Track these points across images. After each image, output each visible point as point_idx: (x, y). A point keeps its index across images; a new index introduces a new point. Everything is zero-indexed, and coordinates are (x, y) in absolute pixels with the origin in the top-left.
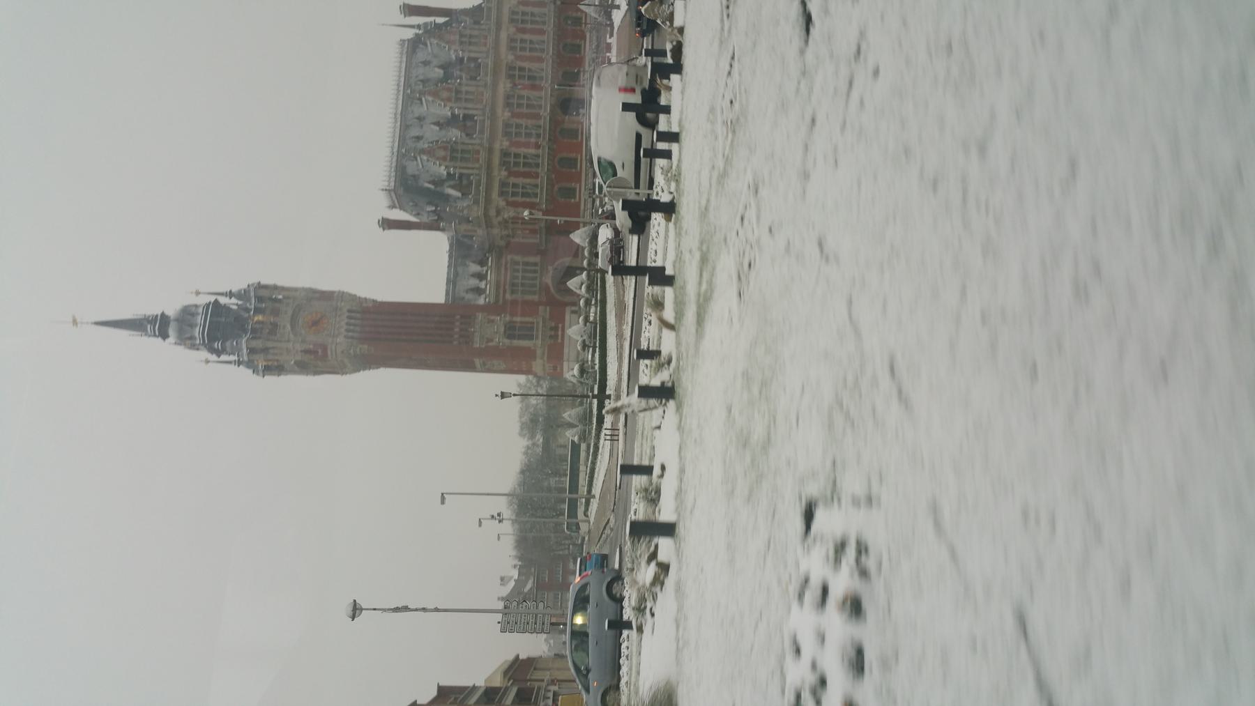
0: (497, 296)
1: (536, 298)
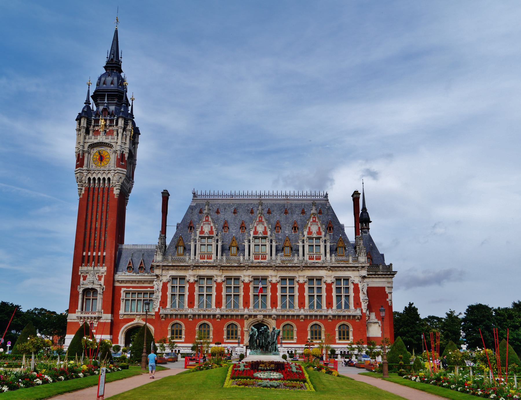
0: (122, 282)
1: (122, 312)
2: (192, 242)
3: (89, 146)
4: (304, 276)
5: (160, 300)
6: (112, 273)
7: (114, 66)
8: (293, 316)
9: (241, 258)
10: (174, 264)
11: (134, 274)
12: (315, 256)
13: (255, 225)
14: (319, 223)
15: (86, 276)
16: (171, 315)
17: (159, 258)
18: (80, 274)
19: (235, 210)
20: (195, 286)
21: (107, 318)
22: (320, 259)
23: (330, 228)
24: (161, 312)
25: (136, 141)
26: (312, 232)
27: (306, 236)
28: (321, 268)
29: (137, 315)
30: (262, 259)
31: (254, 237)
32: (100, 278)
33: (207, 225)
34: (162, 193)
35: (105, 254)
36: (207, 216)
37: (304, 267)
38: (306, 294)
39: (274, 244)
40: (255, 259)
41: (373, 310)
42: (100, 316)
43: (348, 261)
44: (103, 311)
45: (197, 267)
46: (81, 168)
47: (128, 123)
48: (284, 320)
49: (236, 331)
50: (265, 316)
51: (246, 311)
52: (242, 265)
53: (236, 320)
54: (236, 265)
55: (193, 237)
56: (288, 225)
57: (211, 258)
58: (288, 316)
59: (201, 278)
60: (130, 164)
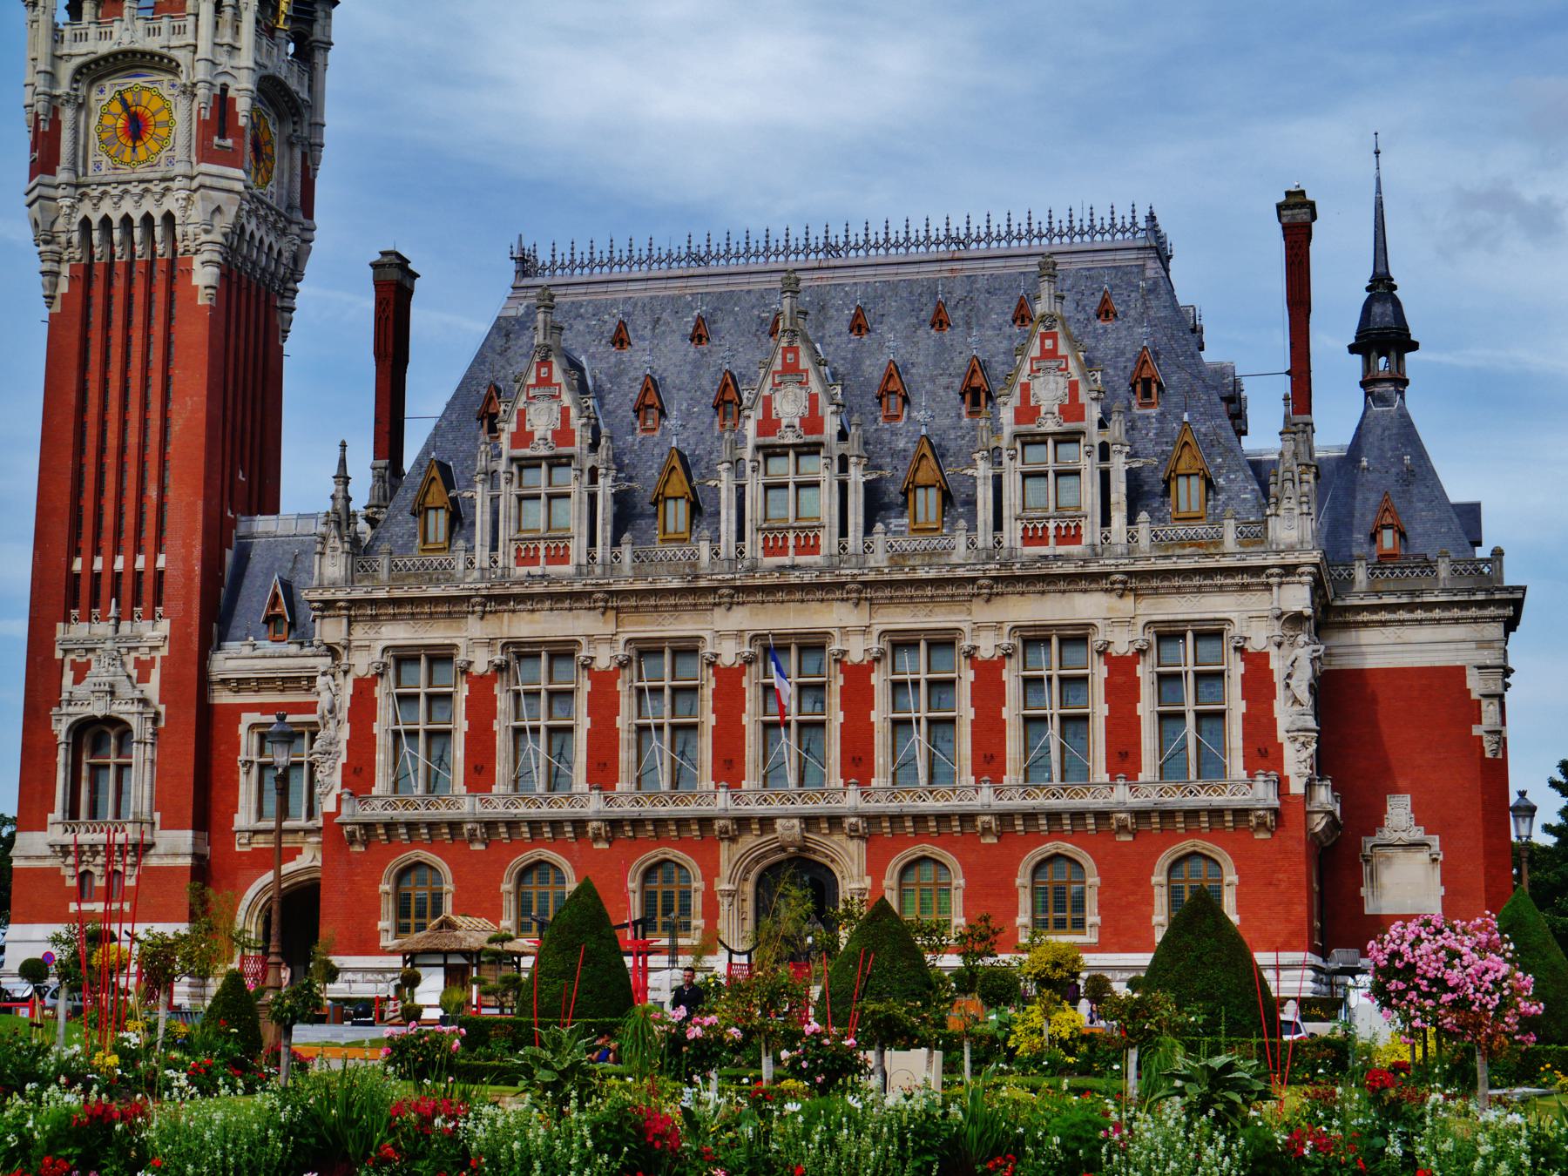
0: (241, 684)
1: (244, 818)
2: (479, 487)
3: (79, 72)
4: (998, 626)
5: (343, 759)
6: (195, 646)
8: (943, 818)
9: (705, 550)
10: (397, 594)
11: (294, 649)
12: (1051, 525)
13: (766, 392)
14: (1072, 364)
15: (88, 665)
16: (390, 826)
17: (334, 567)
18: (59, 655)
19: (700, 321)
20: (497, 689)
21: (175, 846)
22: (1076, 539)
23: (1147, 383)
24: (344, 809)
25: (317, 32)
26: (1037, 409)
27: (1008, 430)
28: (1083, 584)
29: (307, 832)
30: (799, 550)
31: (758, 448)
32: (144, 668)
33: (542, 405)
34: (375, 266)
35: (161, 562)
36: (545, 362)
37: (996, 579)
38: (1012, 712)
39: (856, 477)
40: (769, 551)
41: (1402, 783)
42: (147, 838)
43: (1217, 541)
44: (157, 816)
45: (498, 602)
46: (47, 179)
48: (901, 842)
49: (686, 895)
50: (810, 821)
51: (722, 803)
52: (703, 583)
53: (682, 844)
54: (676, 584)
55: (482, 463)
56: (944, 381)
57: (564, 560)
58: (920, 819)
59: (523, 651)
60: (291, 145)
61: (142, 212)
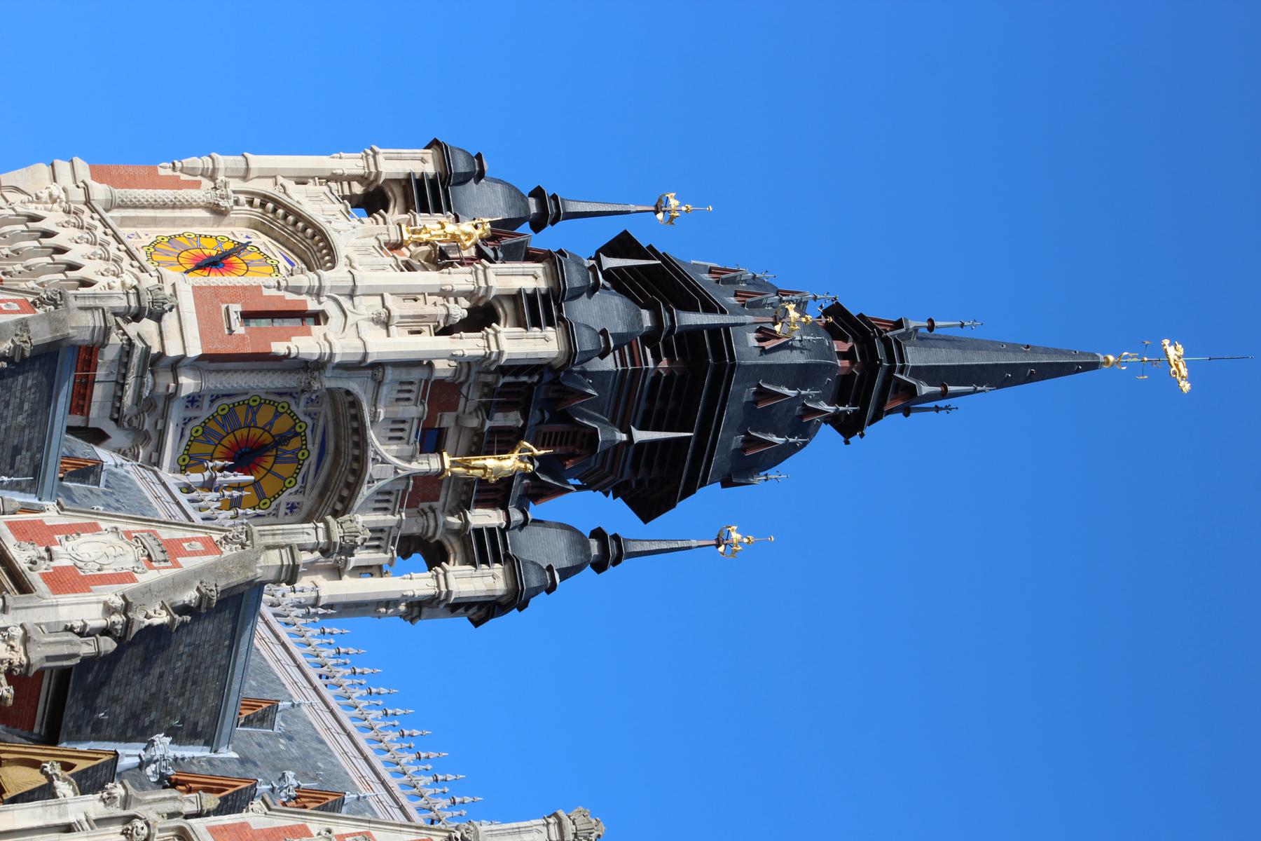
3: (266, 199)
7: (868, 375)
47: (536, 323)
61: (79, 260)
